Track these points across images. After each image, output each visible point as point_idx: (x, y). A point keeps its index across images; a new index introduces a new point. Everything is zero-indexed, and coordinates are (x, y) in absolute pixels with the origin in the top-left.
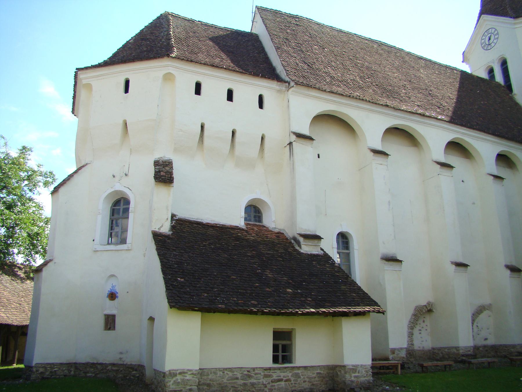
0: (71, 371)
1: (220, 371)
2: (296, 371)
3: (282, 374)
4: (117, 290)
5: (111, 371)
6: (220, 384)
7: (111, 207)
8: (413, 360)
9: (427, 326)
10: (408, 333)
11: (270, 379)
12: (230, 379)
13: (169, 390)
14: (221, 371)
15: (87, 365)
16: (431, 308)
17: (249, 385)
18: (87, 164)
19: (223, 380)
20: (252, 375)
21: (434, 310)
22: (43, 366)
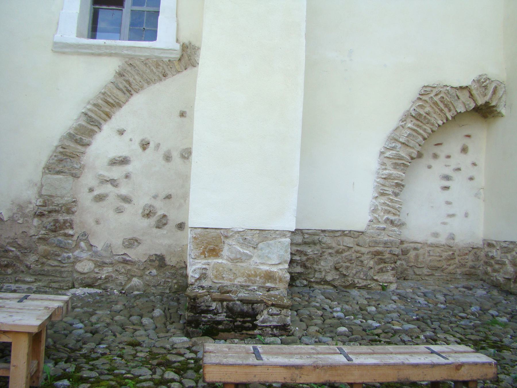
8: (392, 279)
9: (474, 164)
10: (382, 181)
16: (491, 99)
21: (503, 111)
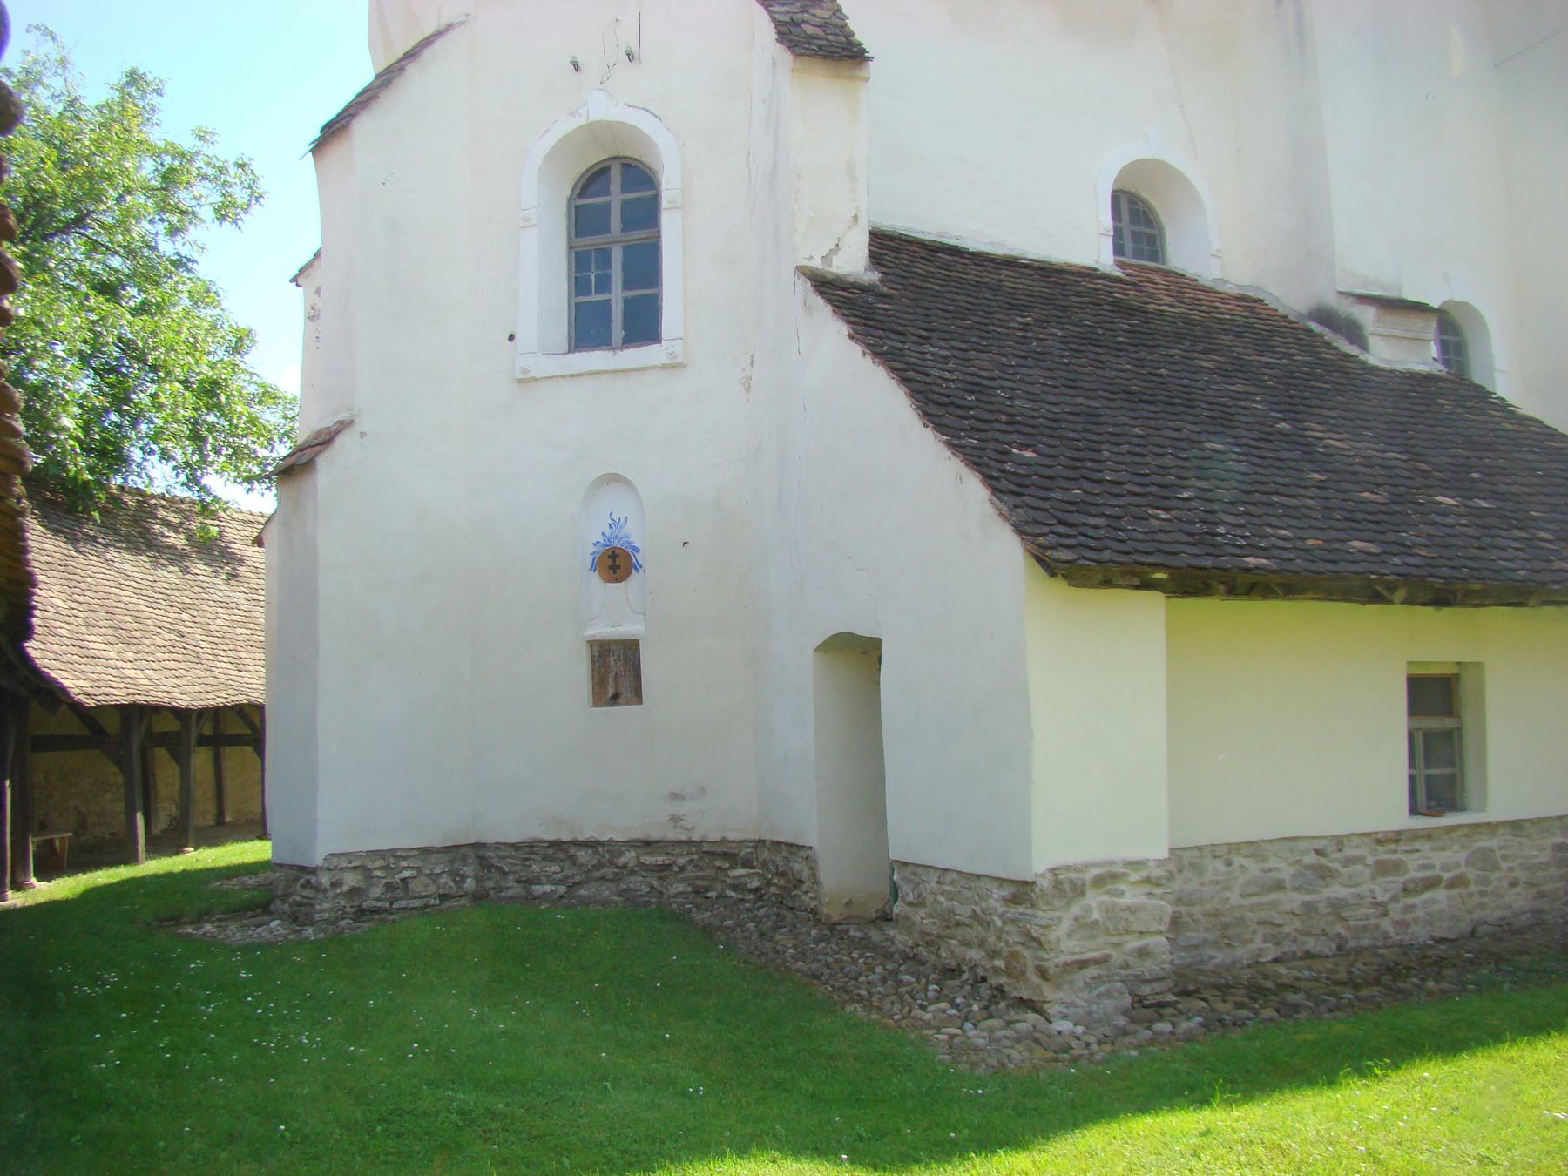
0: (464, 877)
1: (1215, 857)
2: (1485, 842)
3: (1439, 858)
5: (636, 869)
6: (1216, 914)
7: (569, 200)
11: (1397, 878)
12: (1252, 889)
13: (1056, 960)
14: (1220, 857)
15: (529, 848)
17: (1323, 908)
18: (450, 27)
19: (1228, 894)
20: (1334, 865)
22: (354, 864)
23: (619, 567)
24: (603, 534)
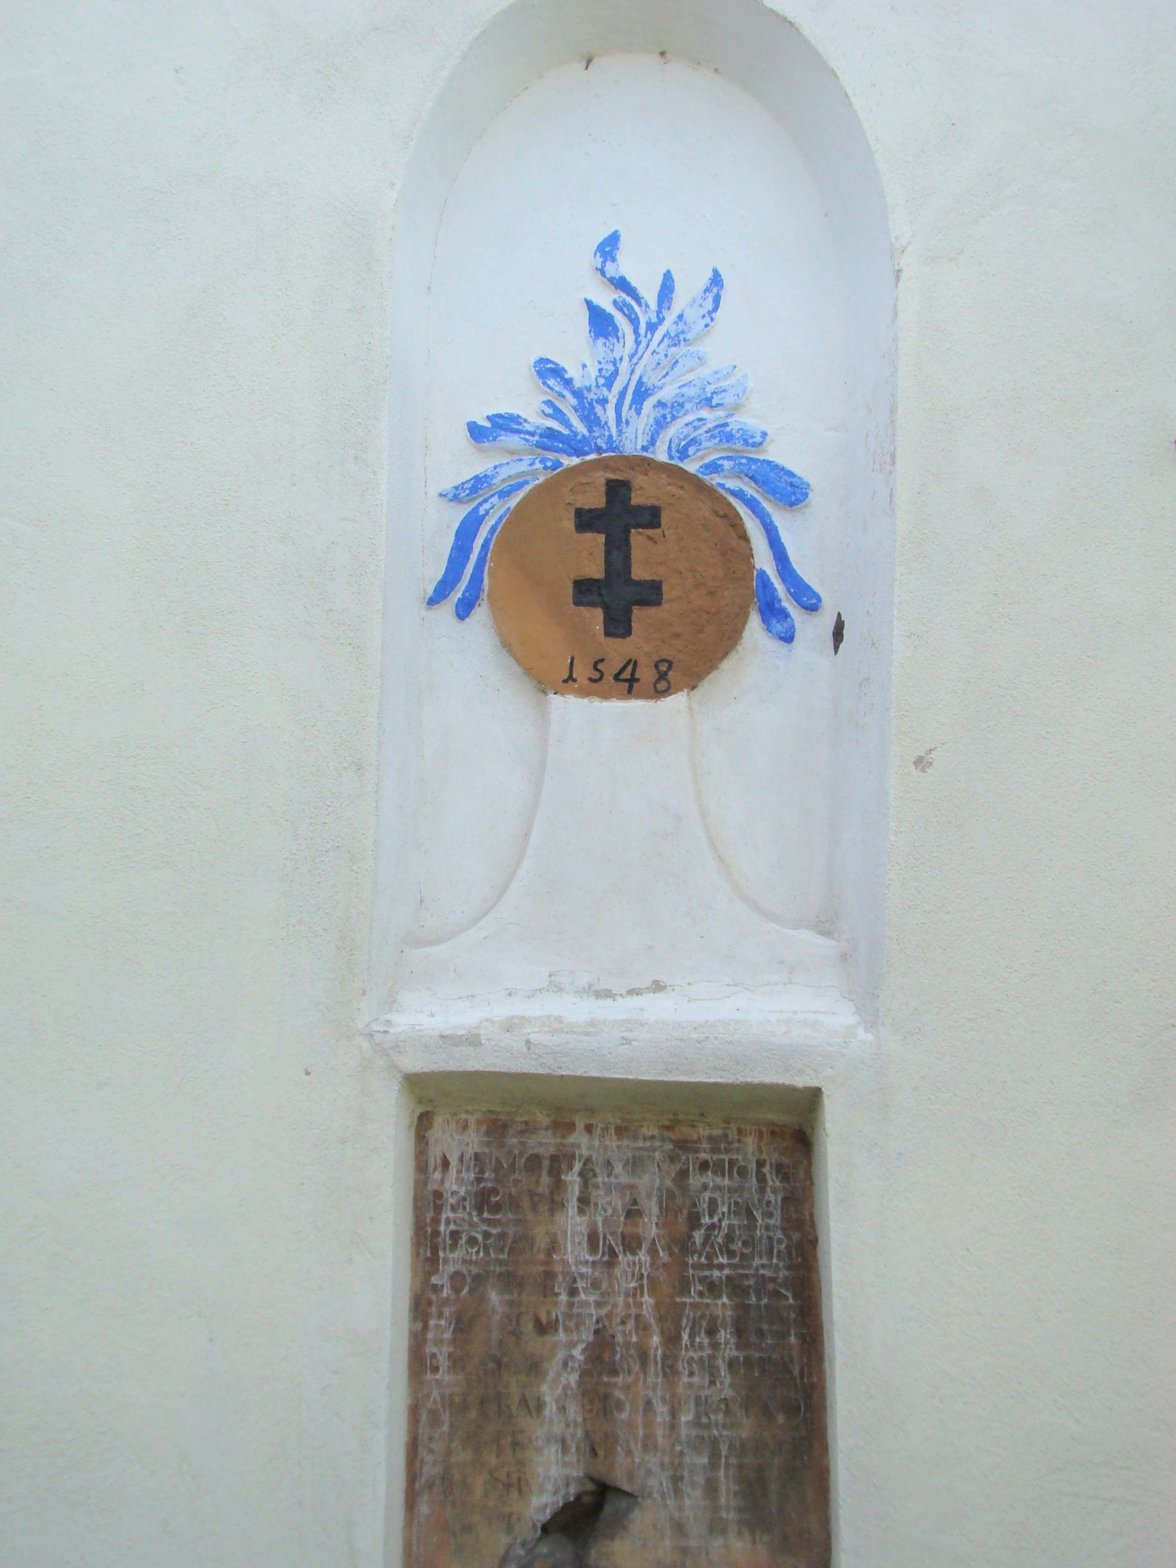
4: (748, 420)
23: (651, 594)
24: (548, 370)
